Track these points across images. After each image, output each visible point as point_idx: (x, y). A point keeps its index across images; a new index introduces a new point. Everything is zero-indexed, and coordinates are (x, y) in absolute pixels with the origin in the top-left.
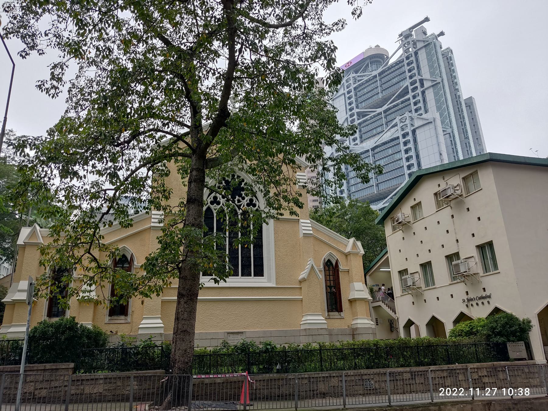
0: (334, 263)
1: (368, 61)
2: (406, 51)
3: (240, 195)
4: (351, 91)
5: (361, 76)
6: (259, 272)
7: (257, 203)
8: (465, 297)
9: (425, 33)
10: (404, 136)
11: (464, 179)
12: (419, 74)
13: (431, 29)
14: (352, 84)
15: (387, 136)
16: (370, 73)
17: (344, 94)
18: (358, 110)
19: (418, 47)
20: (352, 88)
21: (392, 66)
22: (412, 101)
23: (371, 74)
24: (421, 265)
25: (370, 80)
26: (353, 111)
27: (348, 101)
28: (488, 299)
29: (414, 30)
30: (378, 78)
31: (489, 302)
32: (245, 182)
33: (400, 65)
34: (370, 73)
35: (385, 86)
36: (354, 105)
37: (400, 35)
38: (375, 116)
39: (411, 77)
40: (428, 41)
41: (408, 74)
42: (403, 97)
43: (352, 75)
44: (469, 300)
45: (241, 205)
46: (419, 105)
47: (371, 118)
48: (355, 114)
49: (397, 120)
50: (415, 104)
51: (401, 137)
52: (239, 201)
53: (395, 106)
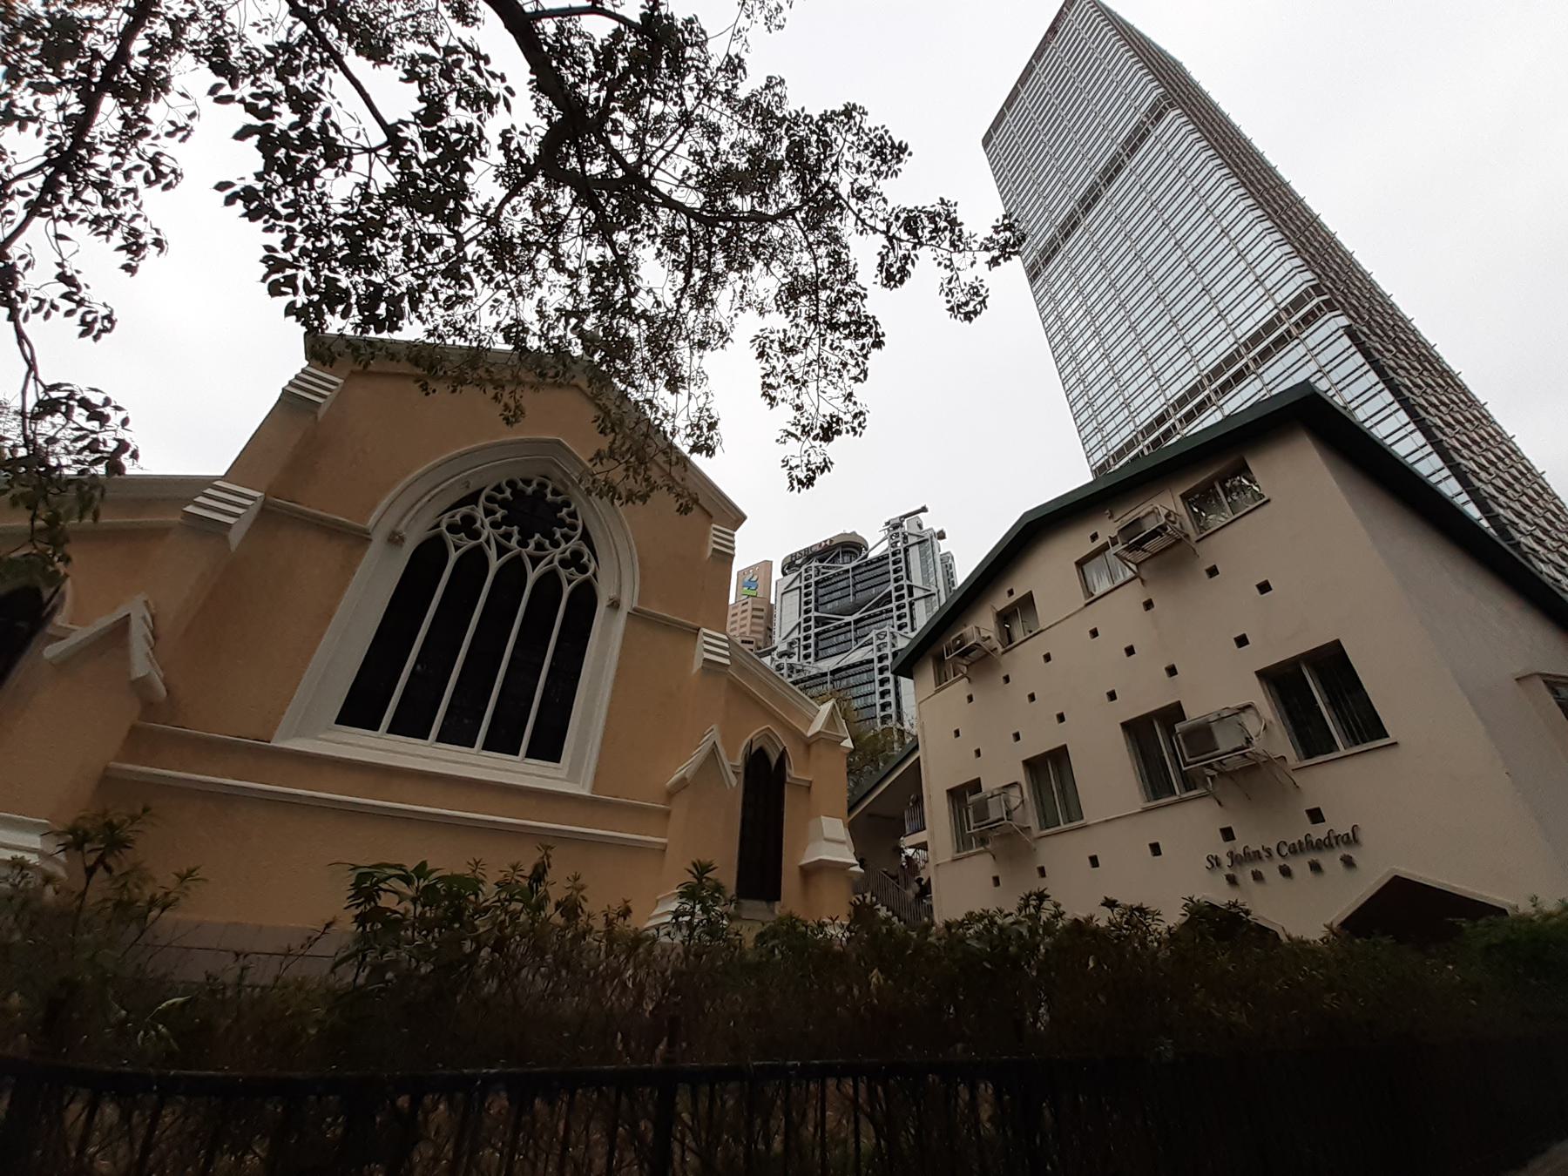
0: (774, 759)
2: (894, 545)
3: (549, 535)
5: (828, 568)
6: (548, 747)
7: (593, 565)
8: (1222, 850)
9: (920, 526)
10: (881, 659)
11: (1184, 497)
12: (908, 578)
13: (929, 522)
15: (856, 656)
17: (800, 588)
18: (817, 614)
19: (910, 542)
20: (812, 581)
21: (872, 562)
22: (895, 613)
24: (1027, 764)
25: (839, 574)
27: (804, 599)
28: (1344, 851)
31: (1348, 862)
32: (573, 507)
35: (859, 587)
36: (812, 606)
37: (888, 523)
38: (839, 627)
39: (896, 580)
41: (893, 576)
44: (1236, 860)
45: (544, 557)
46: (904, 620)
47: (836, 628)
49: (873, 635)
50: (900, 618)
51: (876, 660)
52: (539, 546)
53: (870, 617)
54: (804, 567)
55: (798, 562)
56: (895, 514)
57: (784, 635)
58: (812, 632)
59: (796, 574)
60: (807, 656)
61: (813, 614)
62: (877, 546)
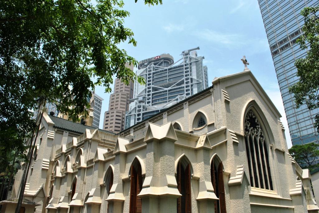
1: (162, 60)
2: (185, 62)
4: (151, 74)
5: (157, 67)
9: (196, 55)
14: (152, 70)
16: (163, 67)
18: (153, 86)
21: (174, 68)
23: (163, 68)
25: (163, 71)
26: (150, 86)
29: (191, 52)
30: (168, 71)
33: (181, 68)
34: (163, 67)
37: (184, 52)
39: (186, 76)
40: (197, 59)
41: (185, 74)
42: (180, 85)
43: (153, 65)
48: (151, 88)
54: (148, 66)
55: (146, 64)
56: (186, 50)
57: (139, 93)
58: (151, 93)
59: (145, 69)
60: (148, 103)
61: (152, 86)
62: (178, 60)
